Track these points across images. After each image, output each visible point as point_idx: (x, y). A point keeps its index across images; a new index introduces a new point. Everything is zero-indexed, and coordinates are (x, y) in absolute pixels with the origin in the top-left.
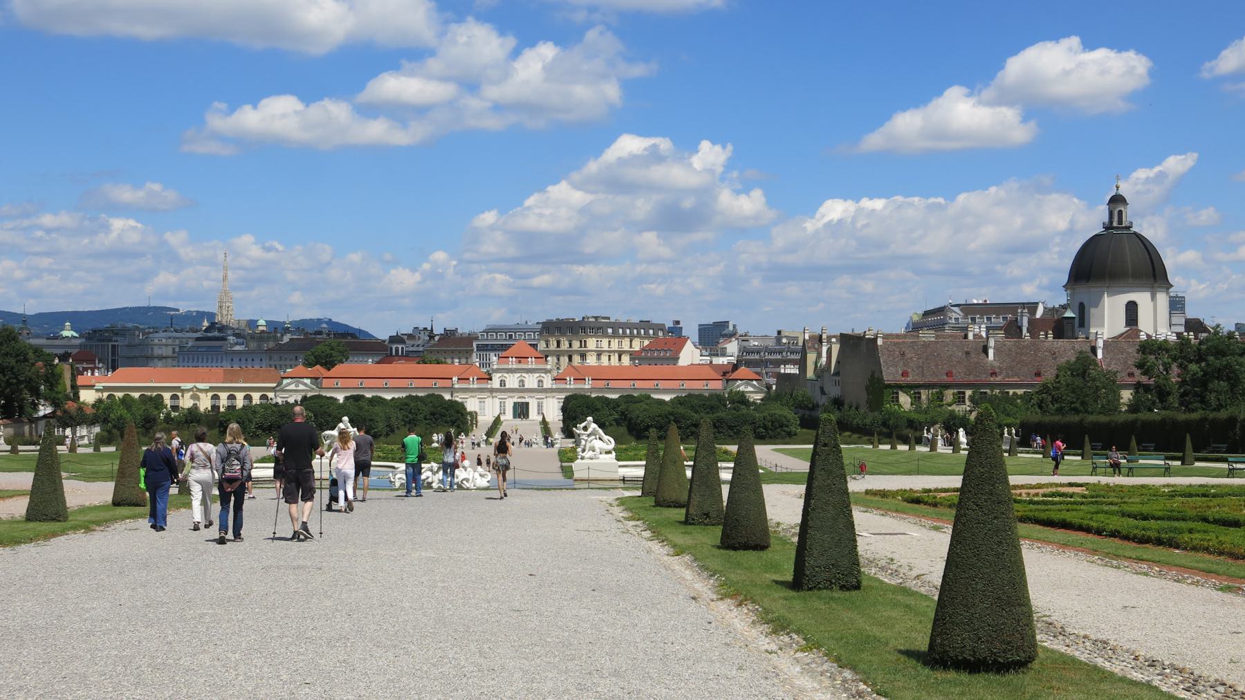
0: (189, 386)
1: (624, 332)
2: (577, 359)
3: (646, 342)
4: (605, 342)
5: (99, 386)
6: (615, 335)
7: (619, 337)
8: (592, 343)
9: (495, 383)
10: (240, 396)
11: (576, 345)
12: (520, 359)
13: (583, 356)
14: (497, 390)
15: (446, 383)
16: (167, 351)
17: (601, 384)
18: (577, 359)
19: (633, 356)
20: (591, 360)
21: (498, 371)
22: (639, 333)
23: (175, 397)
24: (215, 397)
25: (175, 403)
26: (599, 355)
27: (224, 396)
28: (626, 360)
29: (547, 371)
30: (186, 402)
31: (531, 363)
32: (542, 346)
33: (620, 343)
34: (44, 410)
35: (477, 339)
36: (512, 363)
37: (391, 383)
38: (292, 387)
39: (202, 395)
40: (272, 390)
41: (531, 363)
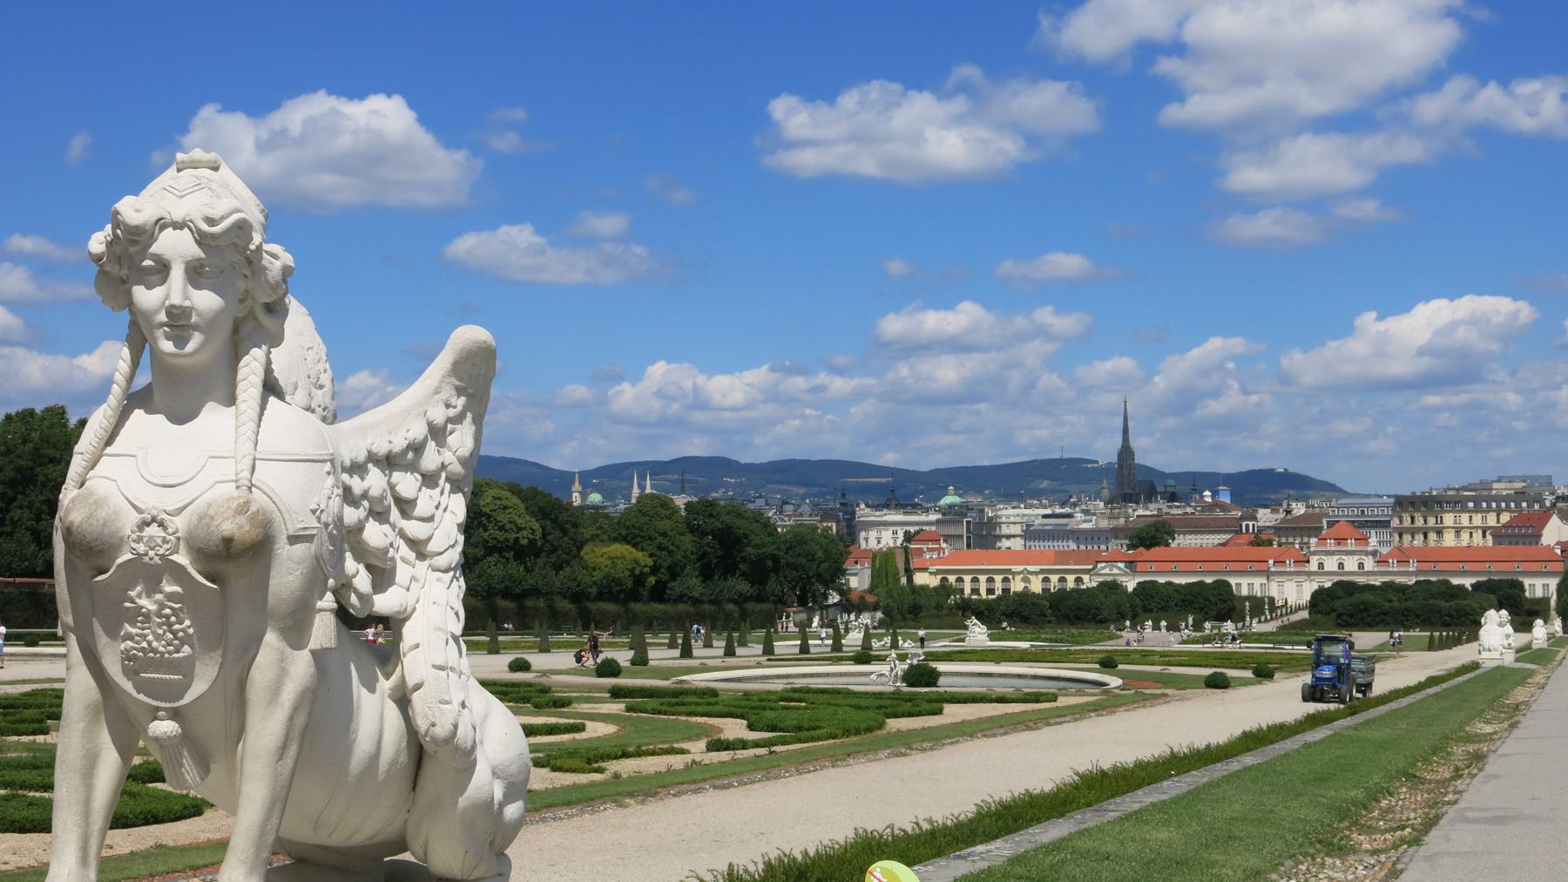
0: (1019, 568)
1: (1489, 506)
2: (1432, 536)
3: (1505, 517)
4: (1464, 519)
5: (933, 569)
6: (1478, 509)
7: (1482, 511)
8: (1449, 519)
9: (1313, 566)
10: (1071, 578)
11: (1431, 521)
12: (1340, 540)
13: (1439, 532)
14: (1315, 573)
15: (1262, 566)
16: (1017, 530)
17: (1425, 566)
18: (1432, 536)
19: (1499, 535)
20: (1449, 540)
21: (1315, 553)
22: (1508, 506)
23: (1006, 580)
24: (1046, 580)
25: (1006, 585)
26: (1458, 531)
27: (1054, 578)
28: (1490, 540)
29: (1367, 553)
30: (1017, 586)
31: (1351, 545)
32: (1395, 522)
33: (1484, 519)
34: (834, 598)
35: (1327, 515)
36: (1331, 545)
37: (1180, 567)
38: (1107, 571)
39: (1032, 578)
40: (1087, 572)
41: (1351, 545)
